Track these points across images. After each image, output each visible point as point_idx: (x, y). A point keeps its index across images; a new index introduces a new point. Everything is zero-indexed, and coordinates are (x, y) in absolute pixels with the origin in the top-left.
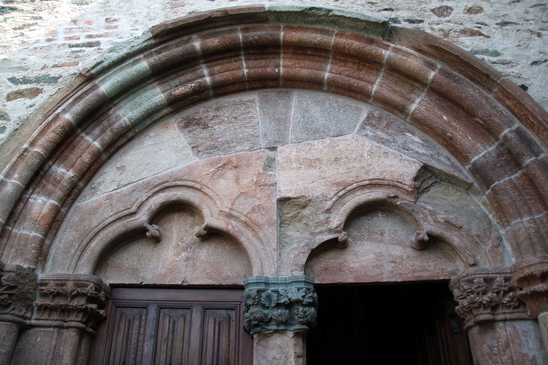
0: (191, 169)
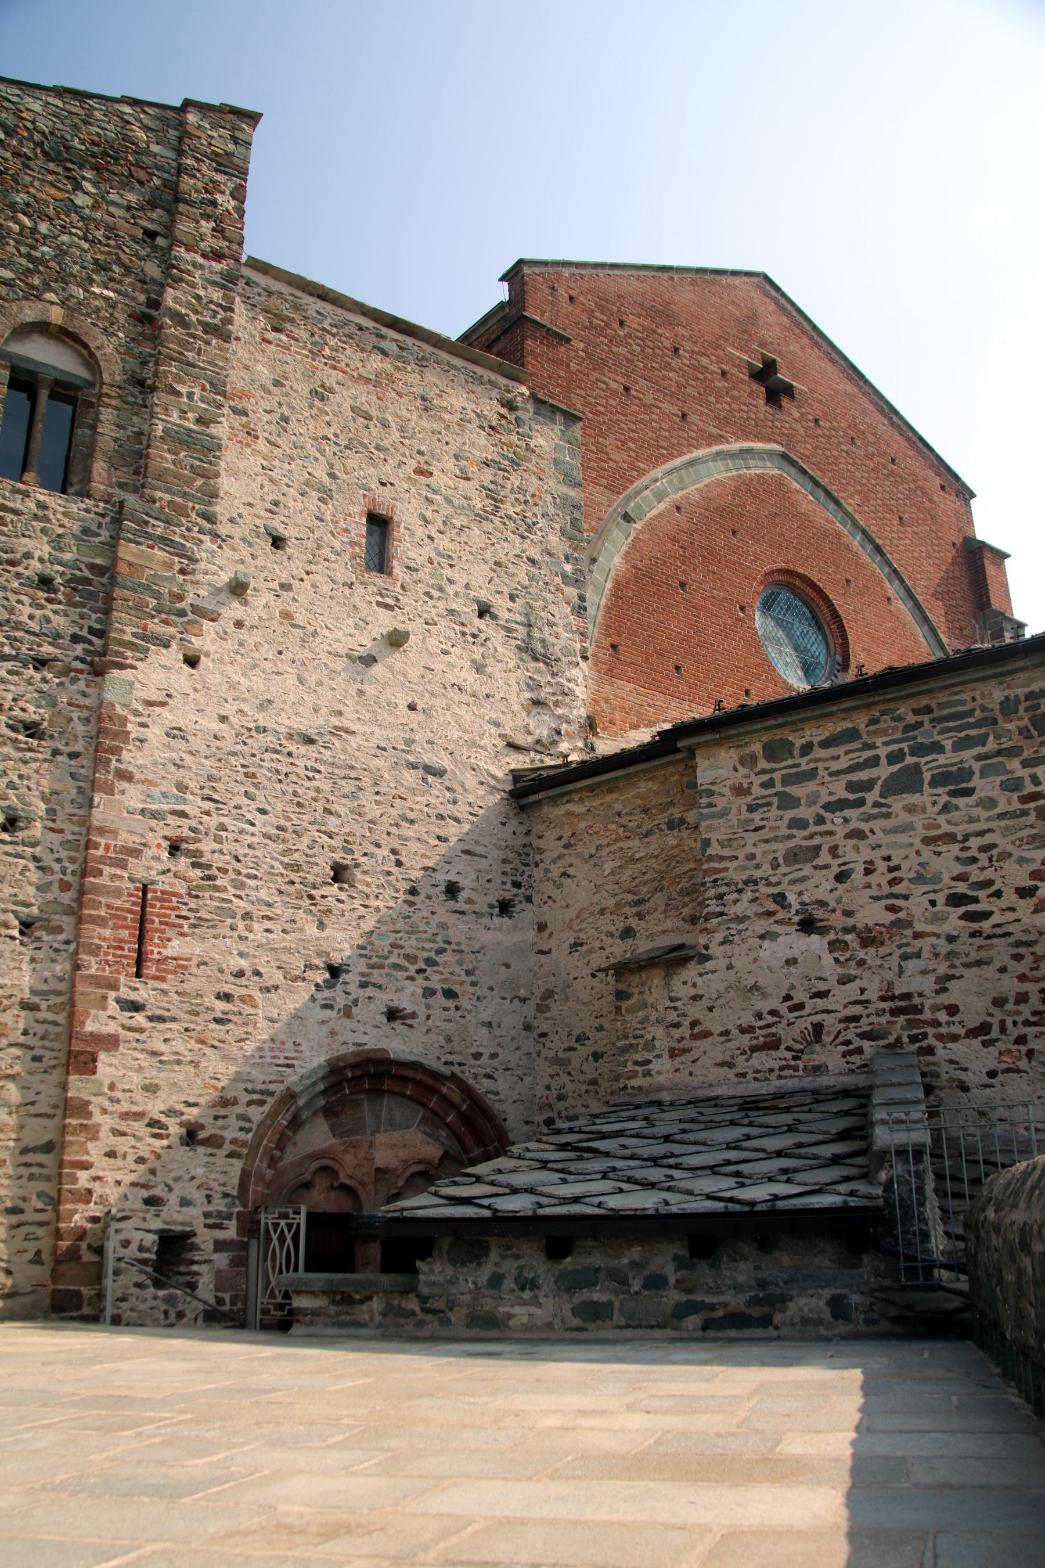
0: (332, 1146)
